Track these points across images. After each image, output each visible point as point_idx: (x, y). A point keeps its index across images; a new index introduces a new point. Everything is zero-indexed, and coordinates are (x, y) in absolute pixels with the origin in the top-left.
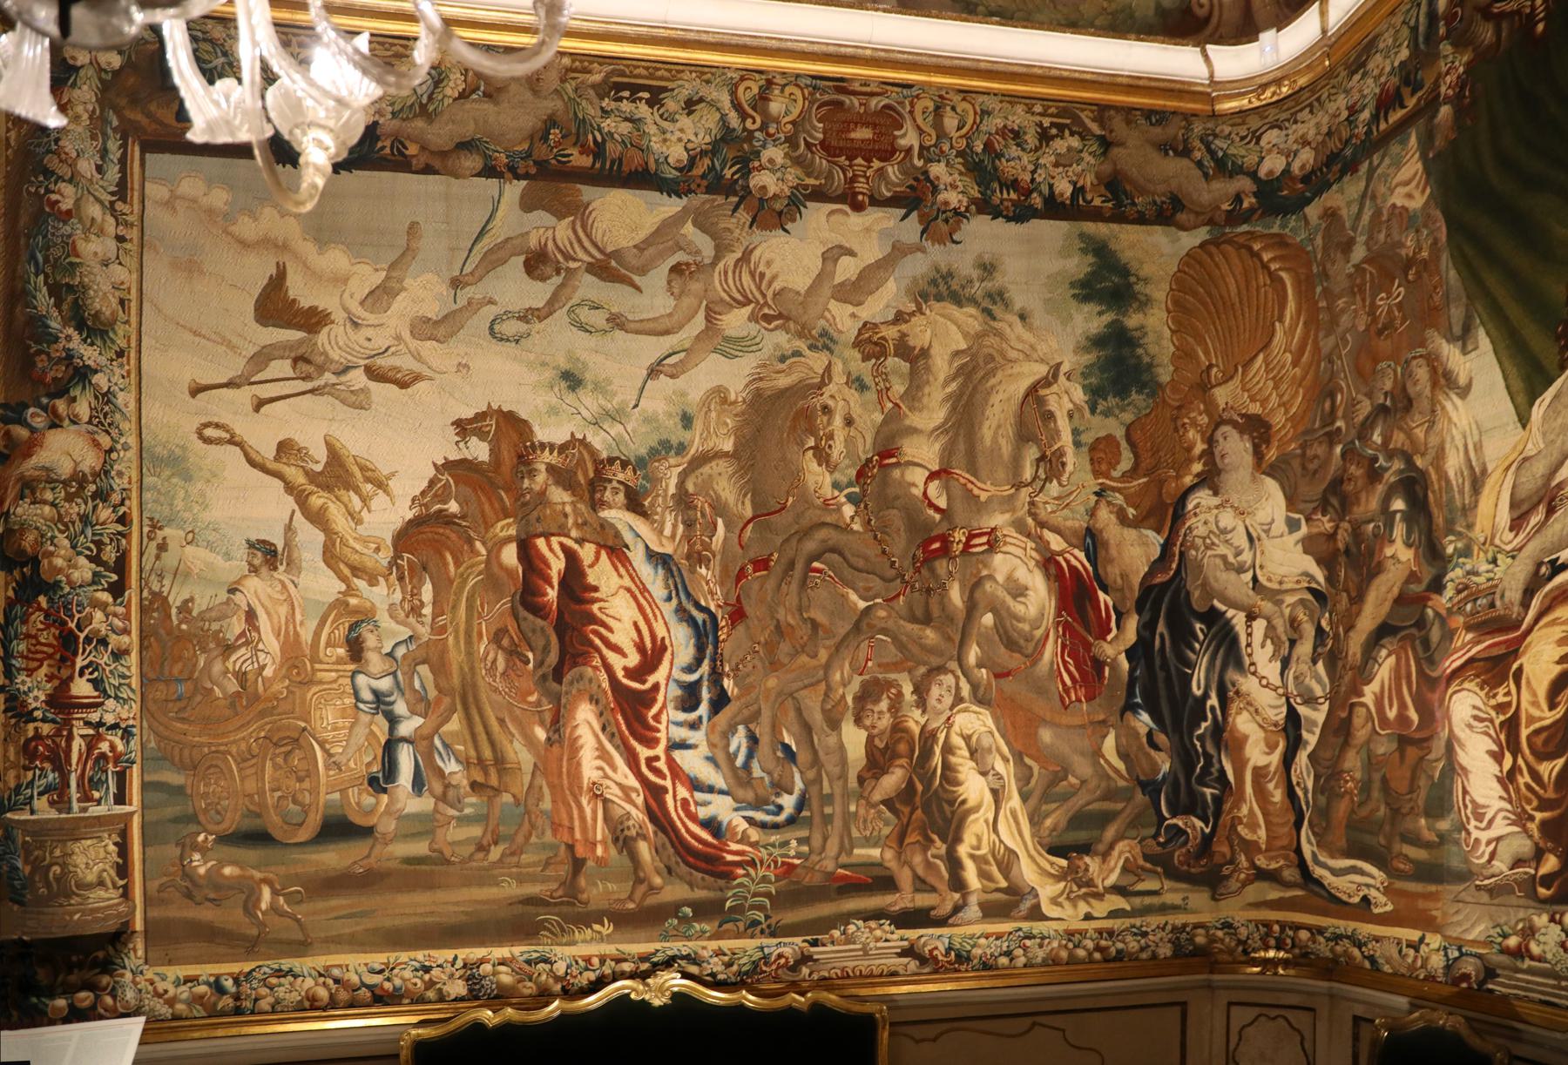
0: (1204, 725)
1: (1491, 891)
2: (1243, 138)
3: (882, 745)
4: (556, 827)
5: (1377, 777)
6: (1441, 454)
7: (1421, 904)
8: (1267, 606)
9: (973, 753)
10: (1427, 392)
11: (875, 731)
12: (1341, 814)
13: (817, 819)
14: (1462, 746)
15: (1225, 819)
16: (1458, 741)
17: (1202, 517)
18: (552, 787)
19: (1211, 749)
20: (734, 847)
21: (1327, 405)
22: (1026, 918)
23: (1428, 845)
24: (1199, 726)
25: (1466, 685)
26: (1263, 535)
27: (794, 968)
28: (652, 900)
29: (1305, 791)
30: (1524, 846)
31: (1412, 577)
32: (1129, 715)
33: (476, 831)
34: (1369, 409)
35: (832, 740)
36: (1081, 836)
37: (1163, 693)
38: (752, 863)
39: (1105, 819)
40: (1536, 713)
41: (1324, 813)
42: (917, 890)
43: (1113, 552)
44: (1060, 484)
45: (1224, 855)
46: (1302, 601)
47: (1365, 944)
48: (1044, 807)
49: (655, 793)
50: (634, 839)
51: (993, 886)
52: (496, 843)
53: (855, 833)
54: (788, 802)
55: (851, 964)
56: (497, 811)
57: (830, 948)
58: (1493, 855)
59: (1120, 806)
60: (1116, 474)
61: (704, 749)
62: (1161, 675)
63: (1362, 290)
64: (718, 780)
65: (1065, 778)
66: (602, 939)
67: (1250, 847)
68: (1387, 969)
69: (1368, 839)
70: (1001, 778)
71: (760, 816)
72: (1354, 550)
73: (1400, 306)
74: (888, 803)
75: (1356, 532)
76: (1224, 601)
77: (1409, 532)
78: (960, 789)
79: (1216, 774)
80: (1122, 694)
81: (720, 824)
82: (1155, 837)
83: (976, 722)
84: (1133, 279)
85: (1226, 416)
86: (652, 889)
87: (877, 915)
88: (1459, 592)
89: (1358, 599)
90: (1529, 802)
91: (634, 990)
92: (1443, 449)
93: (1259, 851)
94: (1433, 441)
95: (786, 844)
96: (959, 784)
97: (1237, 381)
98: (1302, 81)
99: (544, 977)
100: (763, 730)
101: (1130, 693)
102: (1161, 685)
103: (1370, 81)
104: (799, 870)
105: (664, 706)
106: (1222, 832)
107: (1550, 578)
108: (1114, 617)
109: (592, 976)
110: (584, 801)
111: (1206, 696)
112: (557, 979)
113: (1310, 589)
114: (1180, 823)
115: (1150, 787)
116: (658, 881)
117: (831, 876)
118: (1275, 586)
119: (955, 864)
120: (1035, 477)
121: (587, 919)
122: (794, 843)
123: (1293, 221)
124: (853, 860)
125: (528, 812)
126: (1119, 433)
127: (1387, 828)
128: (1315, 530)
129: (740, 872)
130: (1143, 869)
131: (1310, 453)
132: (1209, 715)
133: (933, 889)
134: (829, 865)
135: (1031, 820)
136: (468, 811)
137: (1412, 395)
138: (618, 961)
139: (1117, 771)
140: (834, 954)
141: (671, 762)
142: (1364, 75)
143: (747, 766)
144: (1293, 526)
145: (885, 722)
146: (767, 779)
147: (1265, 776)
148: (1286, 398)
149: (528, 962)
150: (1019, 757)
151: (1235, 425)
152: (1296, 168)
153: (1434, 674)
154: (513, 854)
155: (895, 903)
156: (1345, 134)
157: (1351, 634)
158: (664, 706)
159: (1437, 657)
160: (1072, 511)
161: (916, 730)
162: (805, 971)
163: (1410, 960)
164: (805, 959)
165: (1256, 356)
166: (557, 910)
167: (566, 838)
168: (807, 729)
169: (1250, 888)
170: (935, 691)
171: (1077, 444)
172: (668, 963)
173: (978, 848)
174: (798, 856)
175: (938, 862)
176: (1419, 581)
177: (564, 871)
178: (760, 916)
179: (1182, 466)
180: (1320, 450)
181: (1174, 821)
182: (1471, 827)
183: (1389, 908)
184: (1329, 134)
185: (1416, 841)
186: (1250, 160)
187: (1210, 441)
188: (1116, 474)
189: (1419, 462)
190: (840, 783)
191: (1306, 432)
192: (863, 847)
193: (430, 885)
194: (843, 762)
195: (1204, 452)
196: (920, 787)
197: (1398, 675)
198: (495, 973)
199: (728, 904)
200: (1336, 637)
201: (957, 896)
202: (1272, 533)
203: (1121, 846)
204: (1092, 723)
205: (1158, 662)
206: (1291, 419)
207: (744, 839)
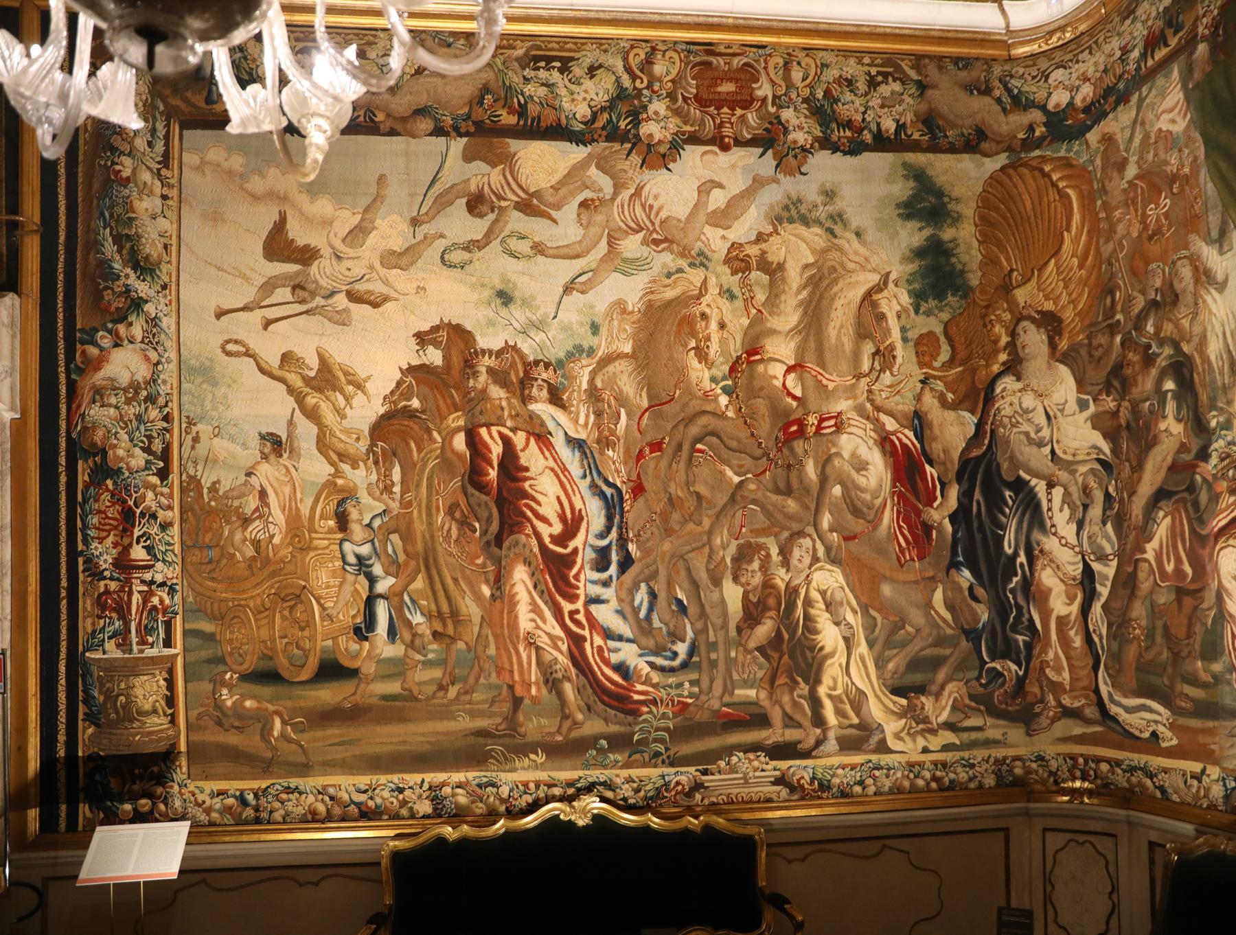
0: (1015, 579)
3: (755, 600)
4: (499, 670)
5: (1159, 624)
9: (828, 606)
11: (749, 588)
12: (1131, 658)
13: (705, 664)
15: (1035, 662)
17: (1008, 399)
18: (496, 636)
20: (639, 687)
22: (875, 751)
23: (1204, 686)
24: (1011, 581)
27: (689, 794)
28: (575, 734)
32: (953, 571)
33: (437, 673)
35: (715, 596)
36: (918, 678)
37: (980, 552)
38: (654, 702)
39: (936, 663)
41: (1116, 657)
42: (786, 726)
43: (937, 431)
48: (887, 653)
49: (577, 641)
50: (561, 681)
51: (847, 722)
52: (453, 684)
53: (736, 676)
54: (682, 648)
55: (735, 791)
56: (453, 656)
57: (717, 777)
59: (948, 651)
61: (614, 604)
62: (978, 536)
64: (625, 629)
65: (903, 627)
66: (537, 767)
70: (852, 627)
71: (659, 661)
74: (761, 649)
78: (819, 637)
79: (1026, 623)
80: (947, 553)
81: (628, 668)
82: (978, 678)
83: (829, 579)
86: (575, 723)
87: (754, 748)
91: (562, 811)
95: (680, 685)
96: (817, 632)
99: (492, 799)
100: (660, 587)
101: (954, 553)
102: (979, 545)
104: (691, 708)
105: (582, 567)
106: (1033, 675)
108: (938, 487)
109: (530, 799)
110: (521, 648)
111: (1016, 554)
112: (503, 801)
114: (998, 667)
115: (972, 635)
116: (580, 717)
117: (717, 714)
119: (816, 703)
121: (524, 750)
122: (687, 685)
124: (735, 700)
125: (477, 657)
129: (645, 709)
130: (969, 707)
132: (1019, 571)
133: (799, 726)
134: (716, 704)
136: (431, 656)
138: (550, 786)
139: (944, 621)
140: (721, 782)
141: (588, 615)
143: (648, 618)
145: (757, 579)
146: (664, 630)
147: (1067, 625)
149: (480, 786)
150: (865, 609)
151: (1033, 320)
154: (466, 693)
155: (769, 738)
158: (582, 567)
161: (782, 586)
162: (698, 797)
164: (698, 786)
166: (501, 741)
167: (507, 679)
168: (695, 585)
170: (796, 553)
172: (589, 789)
173: (834, 689)
174: (690, 696)
175: (803, 701)
177: (506, 707)
178: (661, 748)
181: (993, 665)
185: (1194, 681)
187: (1013, 334)
190: (722, 632)
192: (742, 688)
193: (402, 718)
194: (725, 614)
195: (1008, 343)
196: (786, 636)
198: (454, 795)
199: (636, 737)
201: (818, 731)
203: (950, 687)
204: (923, 579)
205: (975, 525)
207: (647, 681)
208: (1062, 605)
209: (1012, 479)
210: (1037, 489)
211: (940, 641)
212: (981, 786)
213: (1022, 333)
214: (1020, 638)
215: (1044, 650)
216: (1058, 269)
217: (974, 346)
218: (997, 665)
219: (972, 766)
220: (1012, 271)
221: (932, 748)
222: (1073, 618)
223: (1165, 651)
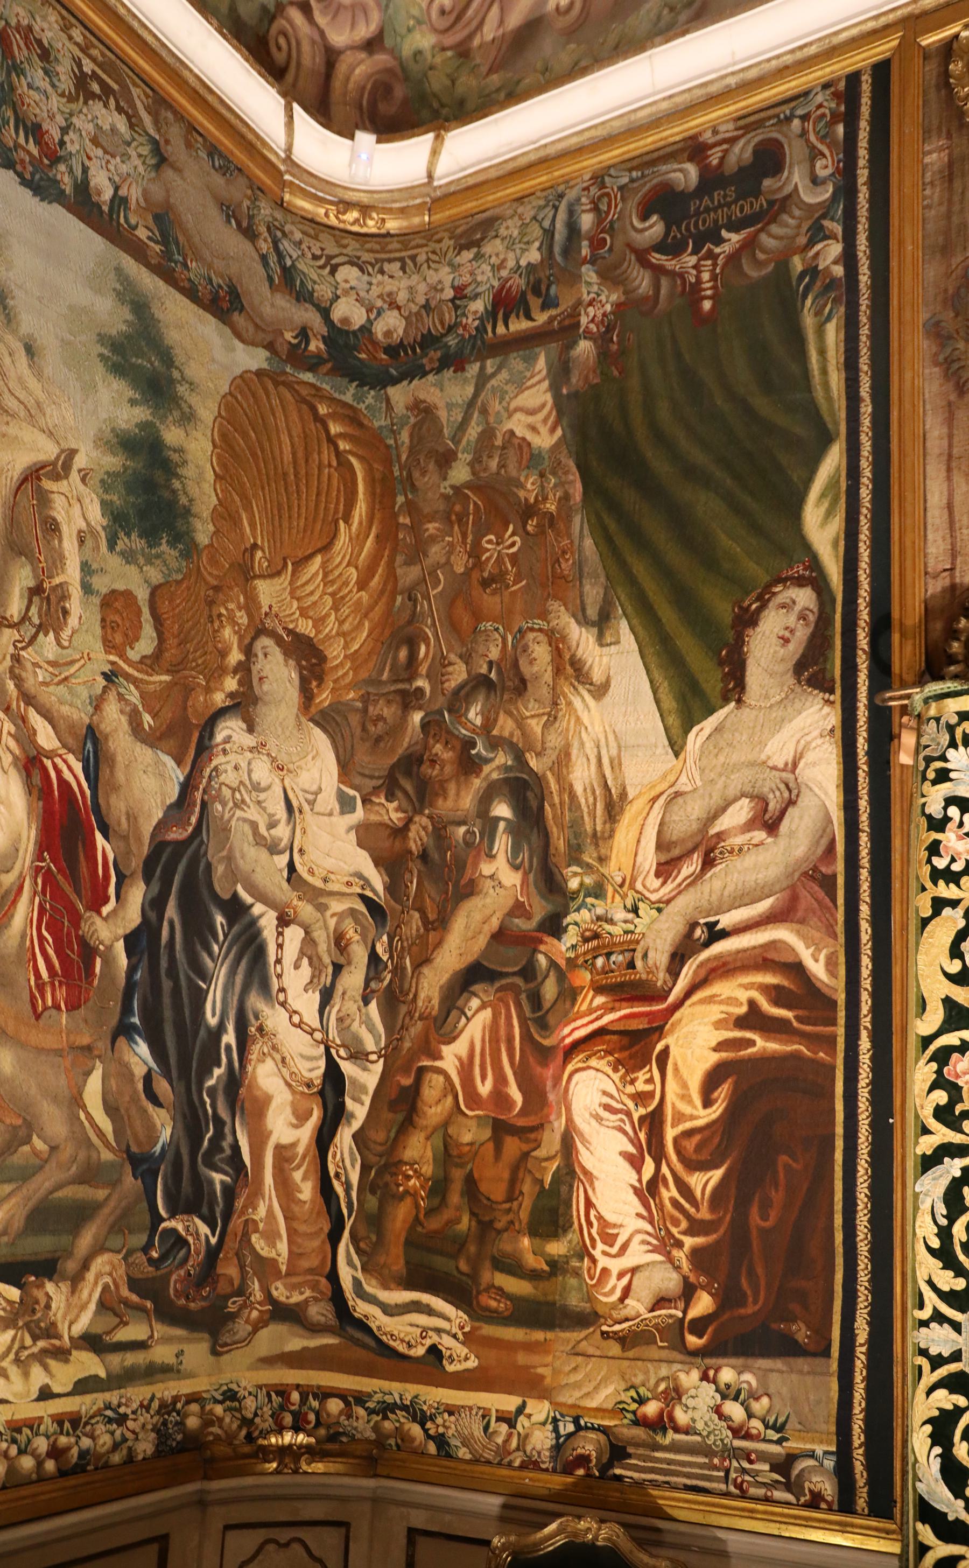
0: (217, 1072)
1: (624, 1340)
2: (315, 257)
5: (458, 1175)
6: (563, 760)
7: (522, 1358)
8: (306, 910)
10: (548, 677)
14: (585, 1142)
16: (581, 1135)
17: (232, 757)
19: (224, 1113)
21: (403, 654)
24: (210, 1073)
25: (593, 1062)
26: (306, 807)
29: (348, 1187)
30: (669, 1281)
31: (518, 909)
32: (122, 1042)
34: (464, 676)
36: (42, 1245)
37: (168, 1014)
40: (686, 1109)
43: (120, 776)
44: (59, 643)
45: (231, 1281)
46: (352, 912)
47: (432, 1418)
58: (626, 1292)
59: (101, 1194)
60: (133, 655)
62: (167, 985)
63: (461, 519)
65: (27, 1140)
67: (266, 1268)
68: (463, 1453)
69: (440, 1263)
72: (435, 856)
73: (514, 558)
75: (440, 830)
77: (516, 849)
80: (115, 1006)
82: (146, 1249)
84: (176, 374)
85: (269, 623)
88: (586, 940)
90: (676, 1223)
92: (568, 755)
93: (278, 1275)
94: (554, 740)
97: (285, 579)
98: (393, 225)
101: (127, 1010)
102: (167, 1000)
103: (486, 268)
107: (707, 944)
108: (113, 880)
111: (221, 1028)
113: (363, 897)
114: (180, 1228)
118: (319, 883)
120: (25, 618)
123: (371, 397)
126: (142, 595)
127: (472, 1249)
128: (374, 818)
130: (126, 1303)
131: (373, 711)
137: (527, 676)
139: (100, 1134)
142: (478, 257)
144: (346, 805)
147: (290, 1160)
148: (346, 627)
151: (279, 641)
152: (379, 329)
153: (546, 1042)
156: (449, 317)
157: (426, 970)
159: (551, 1019)
160: (71, 691)
163: (500, 1440)
165: (309, 558)
169: (264, 1333)
171: (87, 588)
176: (529, 917)
179: (217, 673)
180: (389, 712)
182: (597, 1253)
183: (472, 1363)
184: (426, 307)
186: (323, 291)
187: (248, 651)
188: (133, 655)
189: (533, 763)
191: (371, 682)
195: (240, 663)
197: (493, 1034)
200: (398, 970)
202: (317, 808)
203: (100, 1263)
204: (72, 1048)
205: (164, 964)
206: (353, 657)
209: (226, 896)
210: (262, 922)
212: (130, 1459)
213: (260, 655)
214: (217, 1177)
215: (252, 1203)
216: (326, 575)
218: (178, 1225)
219: (122, 1420)
221: (57, 1389)
222: (301, 1150)
223: (465, 1219)
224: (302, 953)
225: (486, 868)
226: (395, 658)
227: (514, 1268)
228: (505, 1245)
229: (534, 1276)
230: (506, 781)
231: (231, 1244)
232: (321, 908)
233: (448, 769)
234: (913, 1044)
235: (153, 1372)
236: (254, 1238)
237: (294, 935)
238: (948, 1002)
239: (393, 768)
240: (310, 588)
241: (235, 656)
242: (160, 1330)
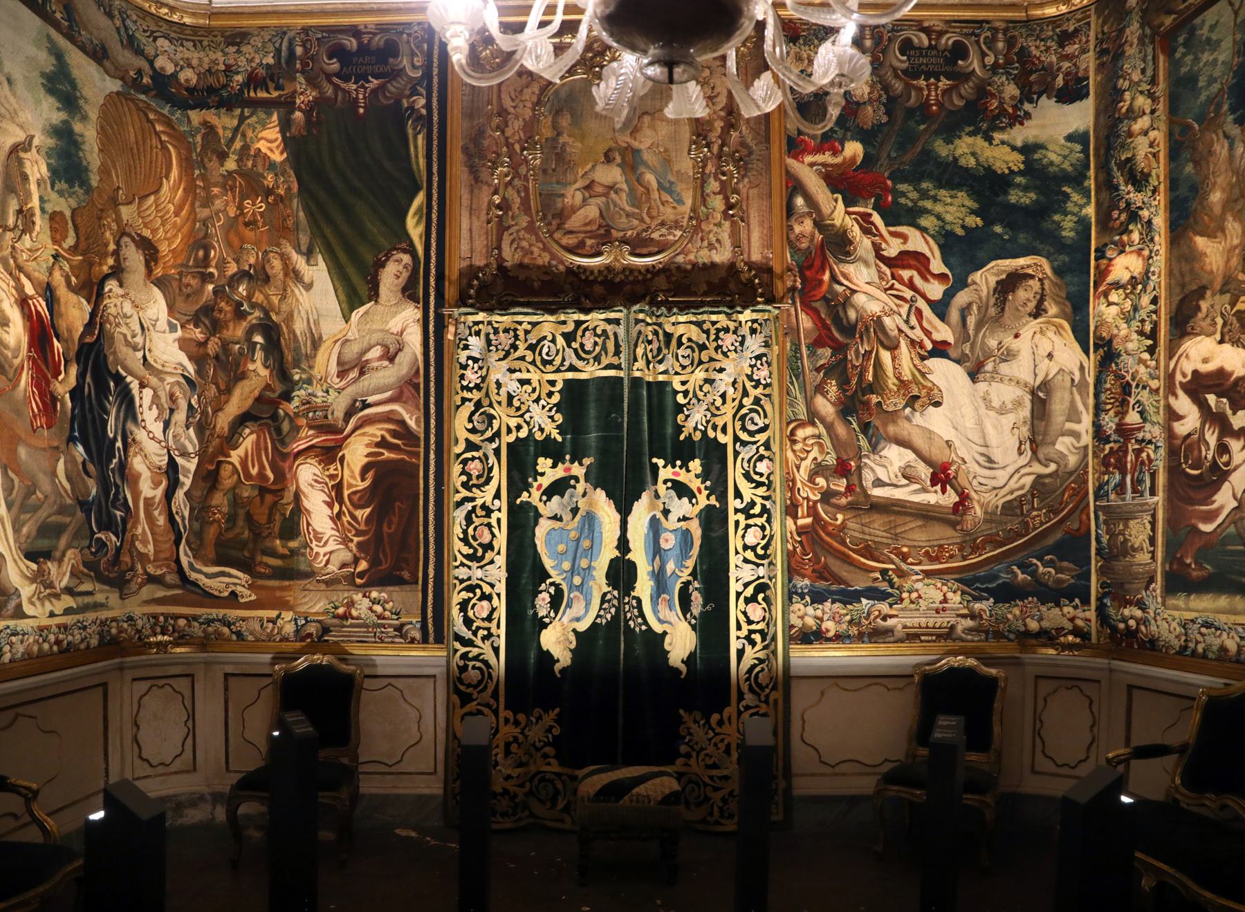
0: (115, 461)
1: (327, 583)
5: (241, 512)
7: (278, 594)
8: (154, 381)
19: (119, 482)
21: (201, 253)
25: (309, 460)
29: (183, 518)
30: (346, 556)
31: (268, 387)
34: (236, 270)
36: (43, 544)
37: (90, 431)
39: (58, 530)
40: (354, 482)
43: (63, 309)
46: (178, 383)
48: (22, 517)
58: (328, 562)
59: (68, 520)
62: (89, 416)
65: (34, 493)
68: (250, 638)
72: (223, 357)
75: (225, 345)
76: (125, 368)
77: (266, 358)
80: (67, 426)
82: (89, 547)
85: (127, 230)
89: (228, 391)
90: (350, 531)
93: (149, 561)
97: (134, 207)
101: (72, 429)
107: (362, 409)
111: (115, 439)
115: (84, 505)
118: (160, 367)
127: (251, 546)
128: (187, 336)
130: (82, 572)
135: (13, 528)
144: (173, 328)
148: (169, 235)
151: (133, 240)
157: (220, 414)
159: (287, 440)
176: (274, 391)
180: (194, 282)
182: (313, 546)
183: (253, 597)
189: (274, 317)
191: (182, 265)
200: (203, 413)
203: (69, 553)
205: (87, 406)
208: (149, 489)
210: (132, 386)
211: (62, 510)
214: (118, 513)
215: (135, 526)
217: (91, 241)
218: (101, 535)
220: (118, 188)
221: (57, 612)
222: (157, 500)
223: (247, 532)
224: (153, 402)
225: (251, 367)
226: (197, 254)
227: (273, 553)
228: (268, 543)
229: (282, 557)
230: (260, 325)
231: (126, 546)
232: (162, 380)
233: (229, 316)
234: (453, 456)
235: (97, 606)
236: (137, 543)
237: (148, 394)
238: (467, 440)
239: (197, 311)
240: (148, 212)
241: (112, 247)
242: (98, 586)
